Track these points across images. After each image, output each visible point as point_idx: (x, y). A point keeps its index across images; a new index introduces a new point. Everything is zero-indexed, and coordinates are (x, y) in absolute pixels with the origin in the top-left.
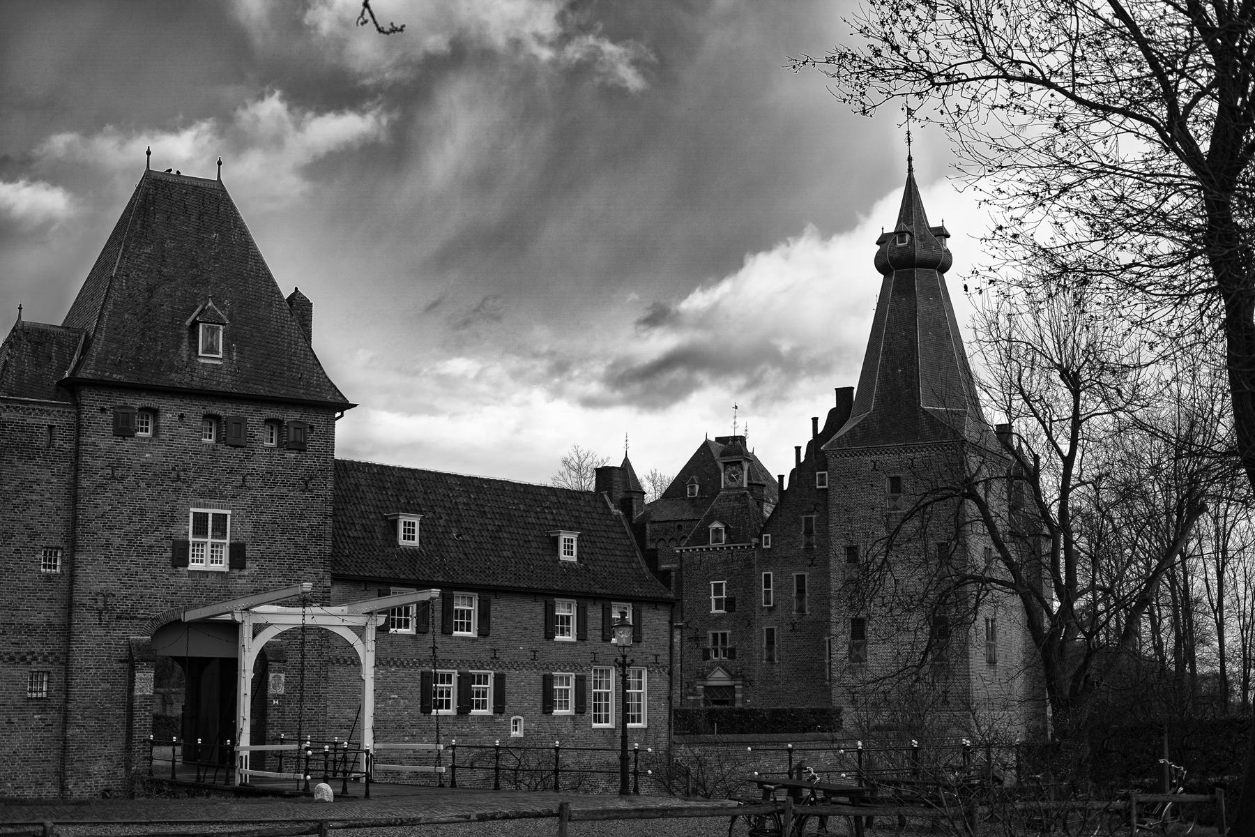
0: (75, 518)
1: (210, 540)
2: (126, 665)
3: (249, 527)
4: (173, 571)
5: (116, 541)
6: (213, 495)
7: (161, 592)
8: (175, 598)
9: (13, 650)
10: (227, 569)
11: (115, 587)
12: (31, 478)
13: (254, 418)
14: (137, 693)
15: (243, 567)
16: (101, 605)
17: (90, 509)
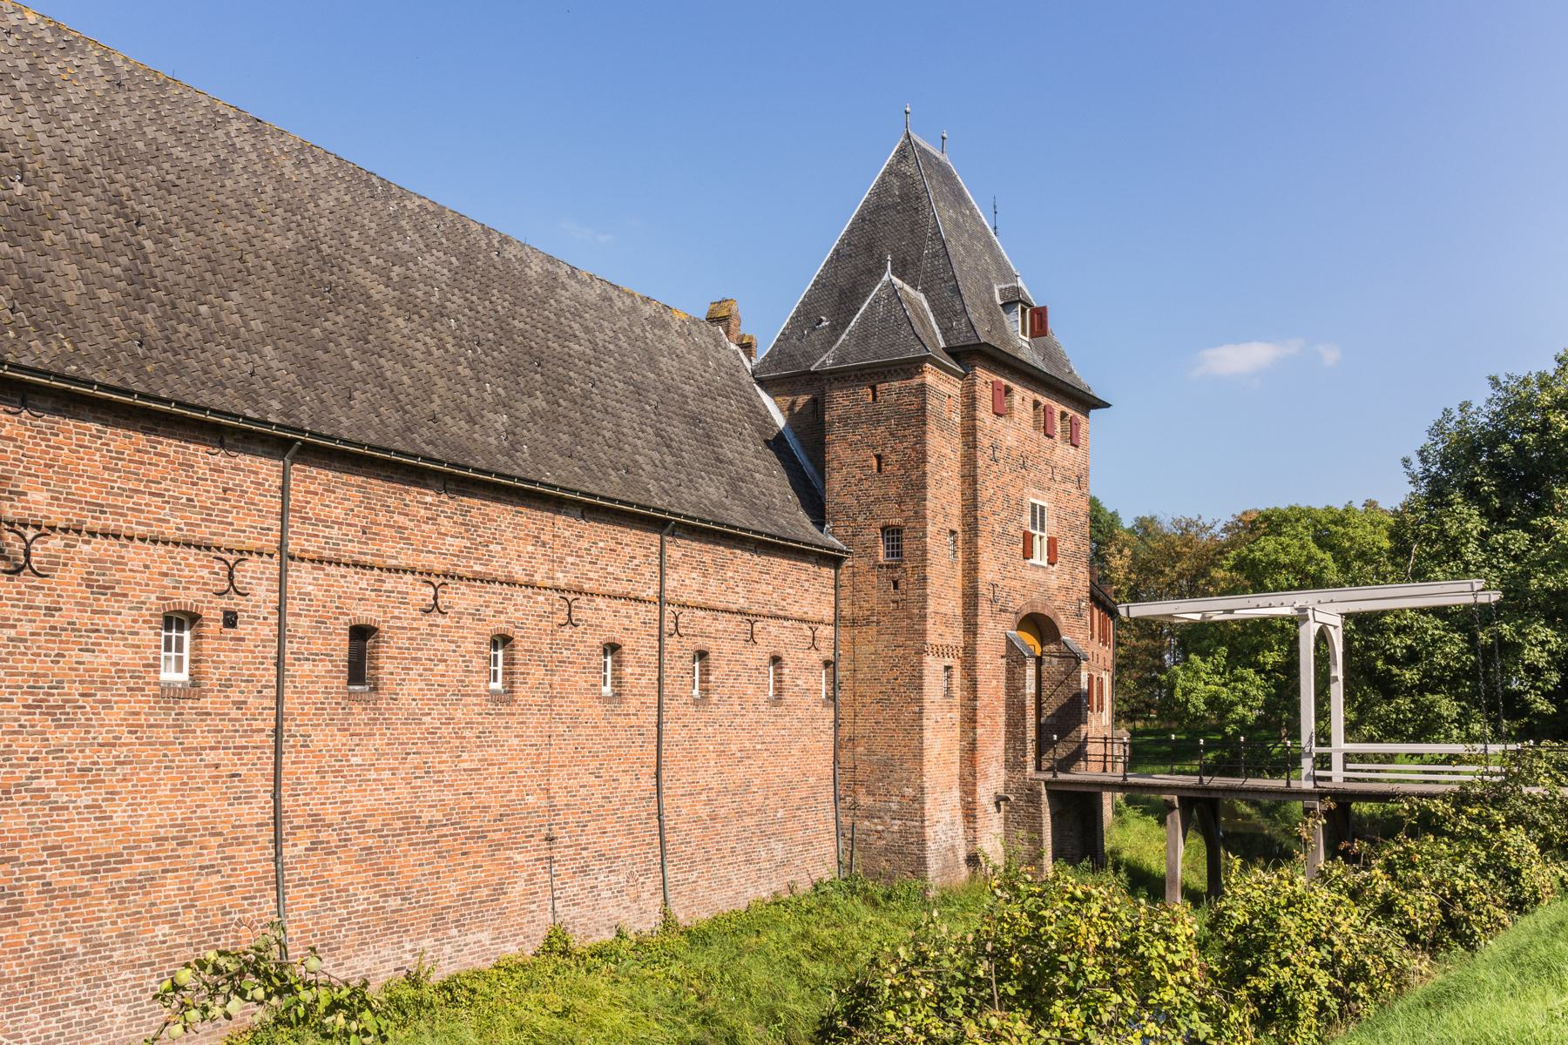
0: (975, 498)
1: (1038, 533)
2: (1004, 661)
3: (1055, 521)
4: (1022, 562)
5: (998, 529)
6: (1039, 485)
7: (1017, 584)
8: (1025, 592)
9: (939, 642)
10: (1045, 563)
11: (996, 577)
12: (944, 451)
13: (1058, 408)
14: (1028, 691)
15: (1053, 564)
16: (991, 596)
17: (984, 492)
